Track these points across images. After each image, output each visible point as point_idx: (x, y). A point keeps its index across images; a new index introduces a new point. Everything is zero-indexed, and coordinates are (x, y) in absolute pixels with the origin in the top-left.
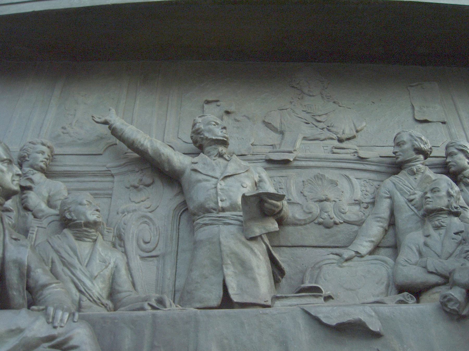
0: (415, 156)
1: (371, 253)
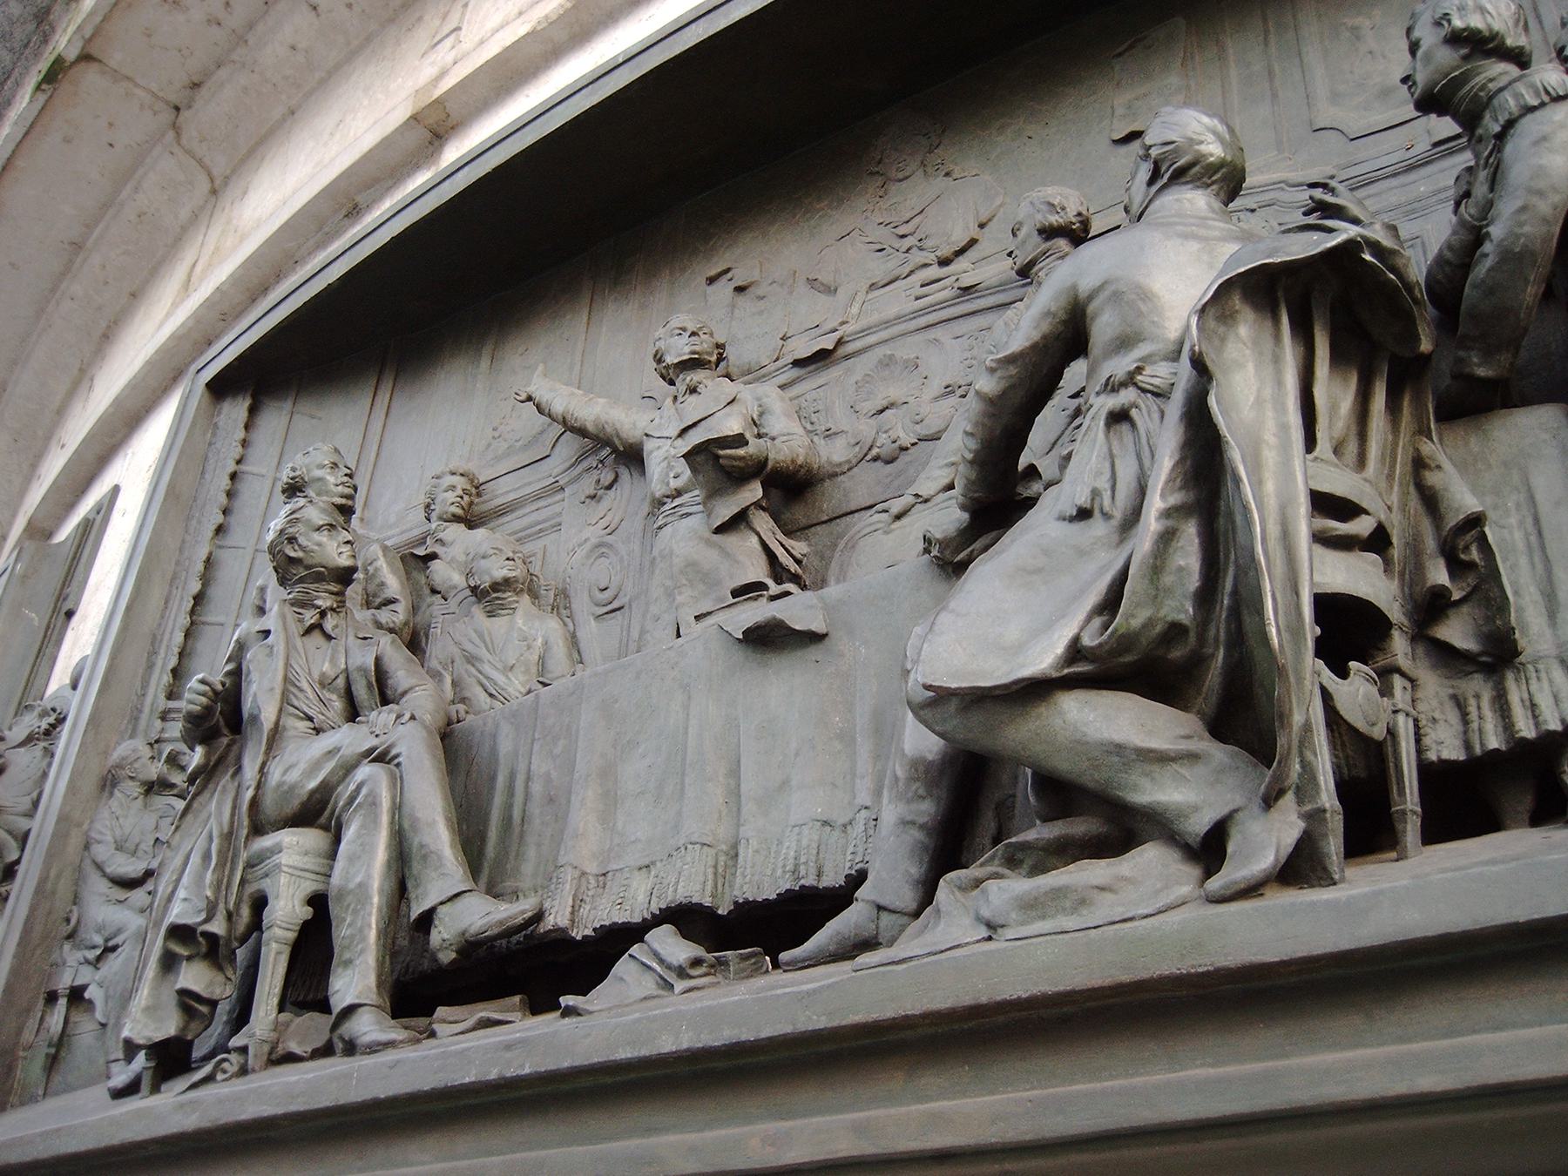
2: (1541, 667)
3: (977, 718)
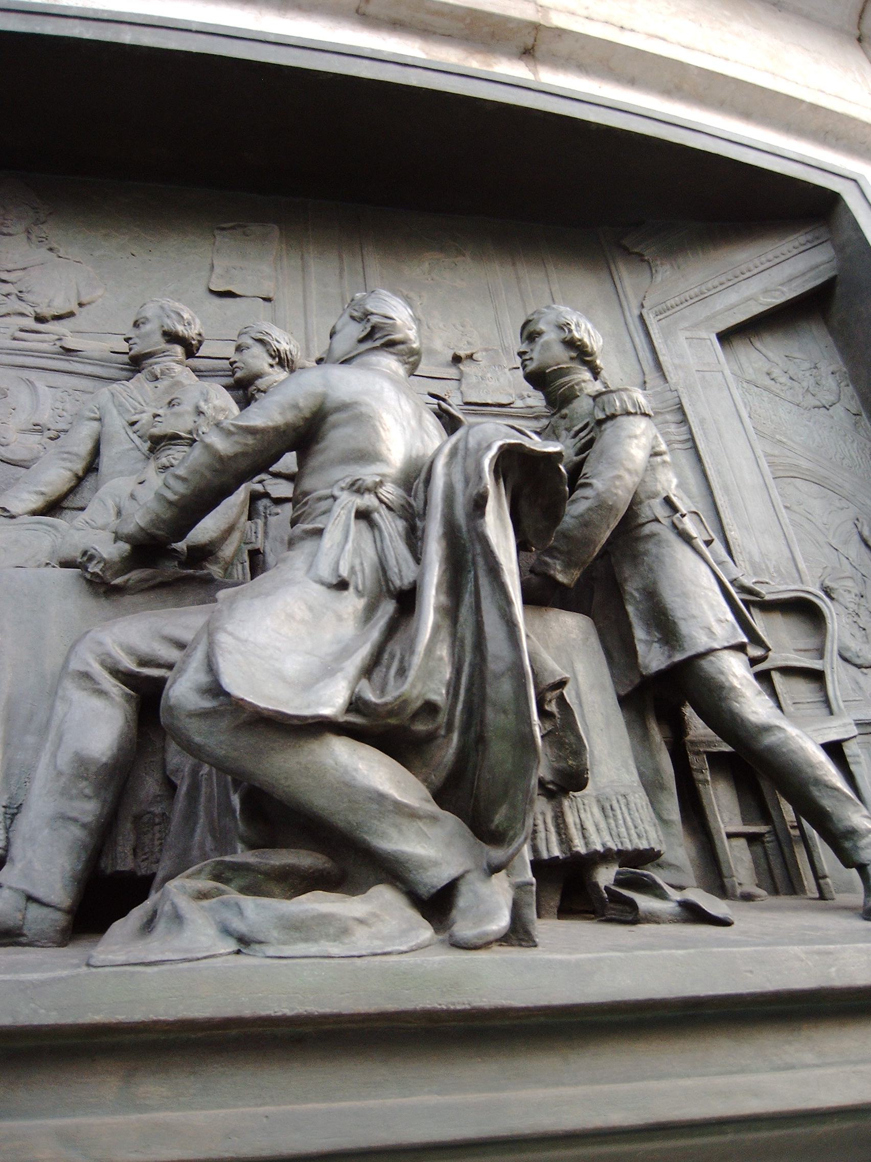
0: (163, 346)
1: (34, 513)
2: (586, 802)
3: (245, 741)
